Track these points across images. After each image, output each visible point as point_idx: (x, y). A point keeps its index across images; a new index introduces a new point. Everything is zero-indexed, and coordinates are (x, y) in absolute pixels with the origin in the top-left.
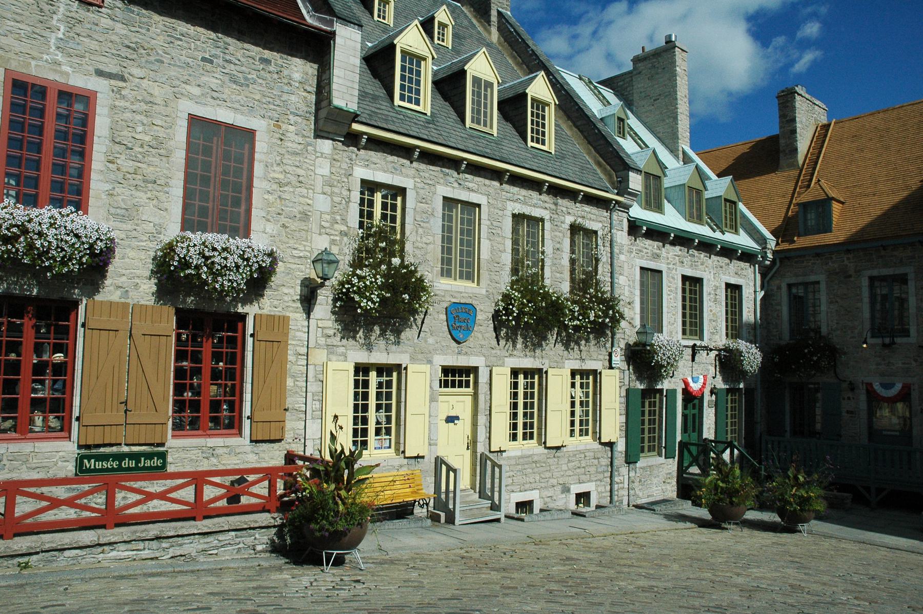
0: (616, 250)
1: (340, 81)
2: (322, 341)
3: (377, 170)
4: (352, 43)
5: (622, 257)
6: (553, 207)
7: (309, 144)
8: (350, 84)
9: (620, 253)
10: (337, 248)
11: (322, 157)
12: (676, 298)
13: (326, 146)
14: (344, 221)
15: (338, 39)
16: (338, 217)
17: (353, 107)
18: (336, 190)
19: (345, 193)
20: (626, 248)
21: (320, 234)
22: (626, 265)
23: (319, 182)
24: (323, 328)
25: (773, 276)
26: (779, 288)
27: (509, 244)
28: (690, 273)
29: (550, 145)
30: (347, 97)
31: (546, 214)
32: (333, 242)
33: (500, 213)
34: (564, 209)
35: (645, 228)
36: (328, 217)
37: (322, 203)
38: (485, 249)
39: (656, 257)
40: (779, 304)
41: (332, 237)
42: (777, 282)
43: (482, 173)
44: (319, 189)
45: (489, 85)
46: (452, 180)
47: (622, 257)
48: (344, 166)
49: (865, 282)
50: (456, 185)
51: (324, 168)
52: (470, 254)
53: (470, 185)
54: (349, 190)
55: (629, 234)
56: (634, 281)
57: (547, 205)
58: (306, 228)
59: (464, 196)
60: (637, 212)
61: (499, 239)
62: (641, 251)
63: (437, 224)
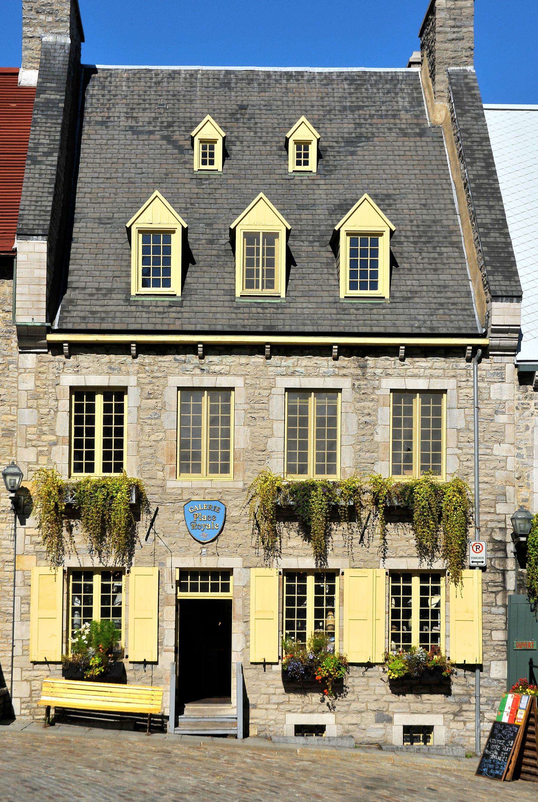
0: (486, 410)
1: (24, 298)
2: (30, 548)
3: (89, 374)
4: (37, 256)
6: (359, 372)
7: (12, 363)
8: (35, 298)
10: (46, 458)
11: (25, 372)
13: (30, 360)
14: (53, 432)
15: (20, 257)
16: (45, 428)
17: (41, 319)
18: (42, 402)
19: (53, 403)
21: (26, 447)
22: (509, 430)
23: (24, 397)
24: (31, 536)
27: (280, 429)
29: (383, 289)
30: (34, 312)
31: (345, 384)
32: (40, 454)
33: (265, 393)
34: (378, 371)
36: (34, 430)
37: (28, 417)
38: (239, 437)
41: (39, 448)
43: (235, 350)
44: (23, 404)
45: (271, 237)
46: (190, 367)
47: (501, 419)
48: (51, 377)
50: (198, 371)
51: (28, 383)
52: (226, 444)
53: (217, 368)
54: (57, 400)
57: (352, 371)
58: (10, 443)
59: (208, 381)
61: (264, 423)
63: (171, 420)
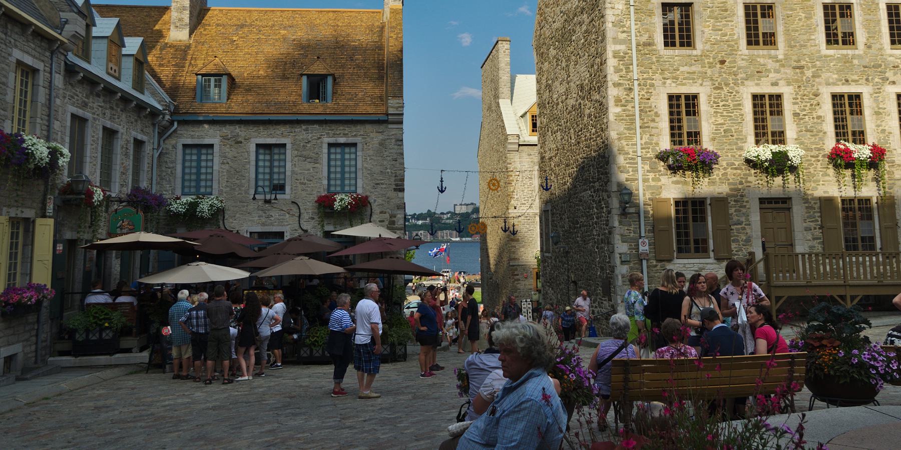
0: (54, 94)
5: (58, 101)
9: (57, 96)
12: (97, 148)
20: (61, 92)
25: (170, 136)
26: (174, 147)
28: (109, 124)
34: (13, 41)
35: (82, 75)
39: (85, 105)
40: (174, 162)
42: (172, 141)
49: (253, 148)
55: (65, 77)
56: (65, 127)
60: (71, 57)
62: (73, 97)
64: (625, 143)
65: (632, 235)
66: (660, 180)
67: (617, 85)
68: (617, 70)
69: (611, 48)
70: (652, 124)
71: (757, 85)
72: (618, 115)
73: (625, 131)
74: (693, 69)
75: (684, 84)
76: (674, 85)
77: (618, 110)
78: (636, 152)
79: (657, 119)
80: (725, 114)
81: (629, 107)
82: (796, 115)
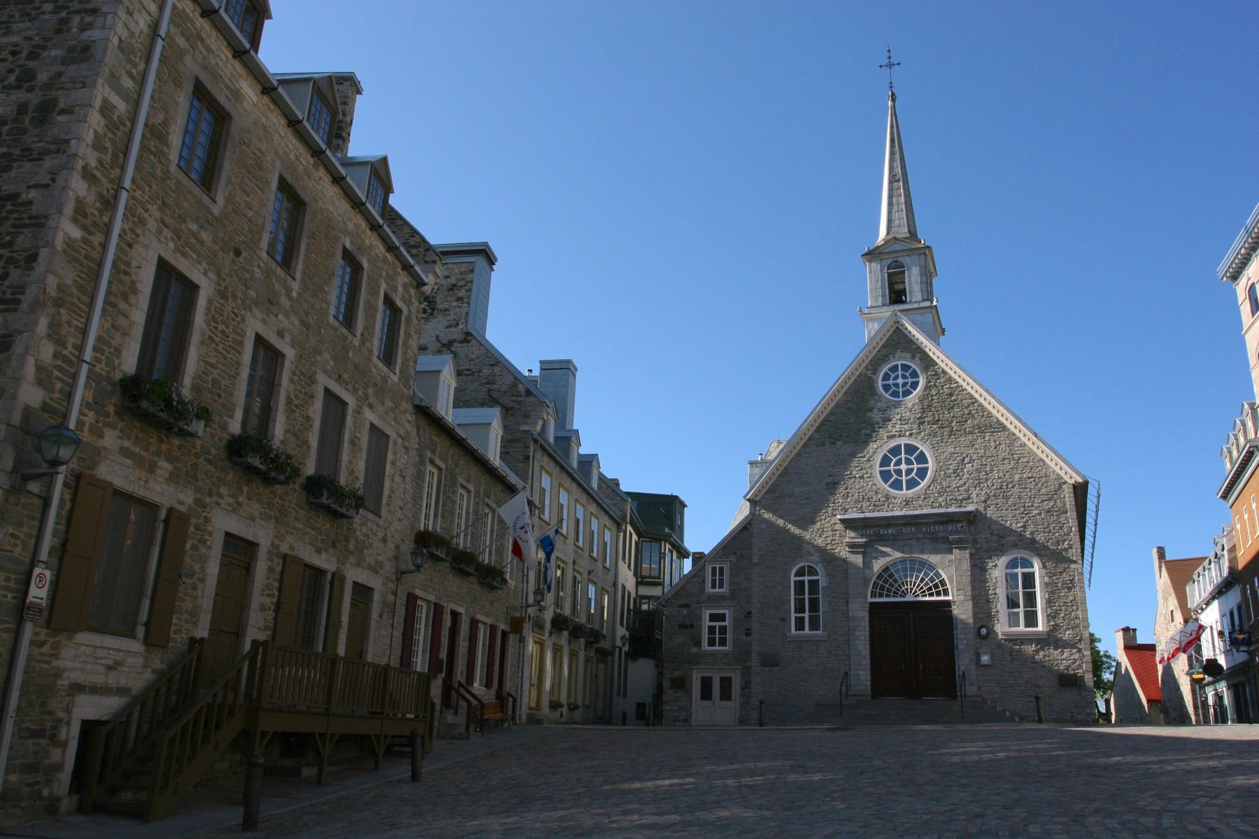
64: (65, 317)
65: (18, 550)
66: (101, 436)
67: (87, 175)
68: (97, 145)
69: (102, 91)
70: (122, 305)
71: (264, 322)
72: (70, 243)
73: (74, 290)
74: (204, 236)
75: (185, 255)
76: (171, 245)
77: (76, 233)
78: (81, 348)
79: (132, 299)
80: (220, 349)
81: (97, 239)
82: (289, 401)
